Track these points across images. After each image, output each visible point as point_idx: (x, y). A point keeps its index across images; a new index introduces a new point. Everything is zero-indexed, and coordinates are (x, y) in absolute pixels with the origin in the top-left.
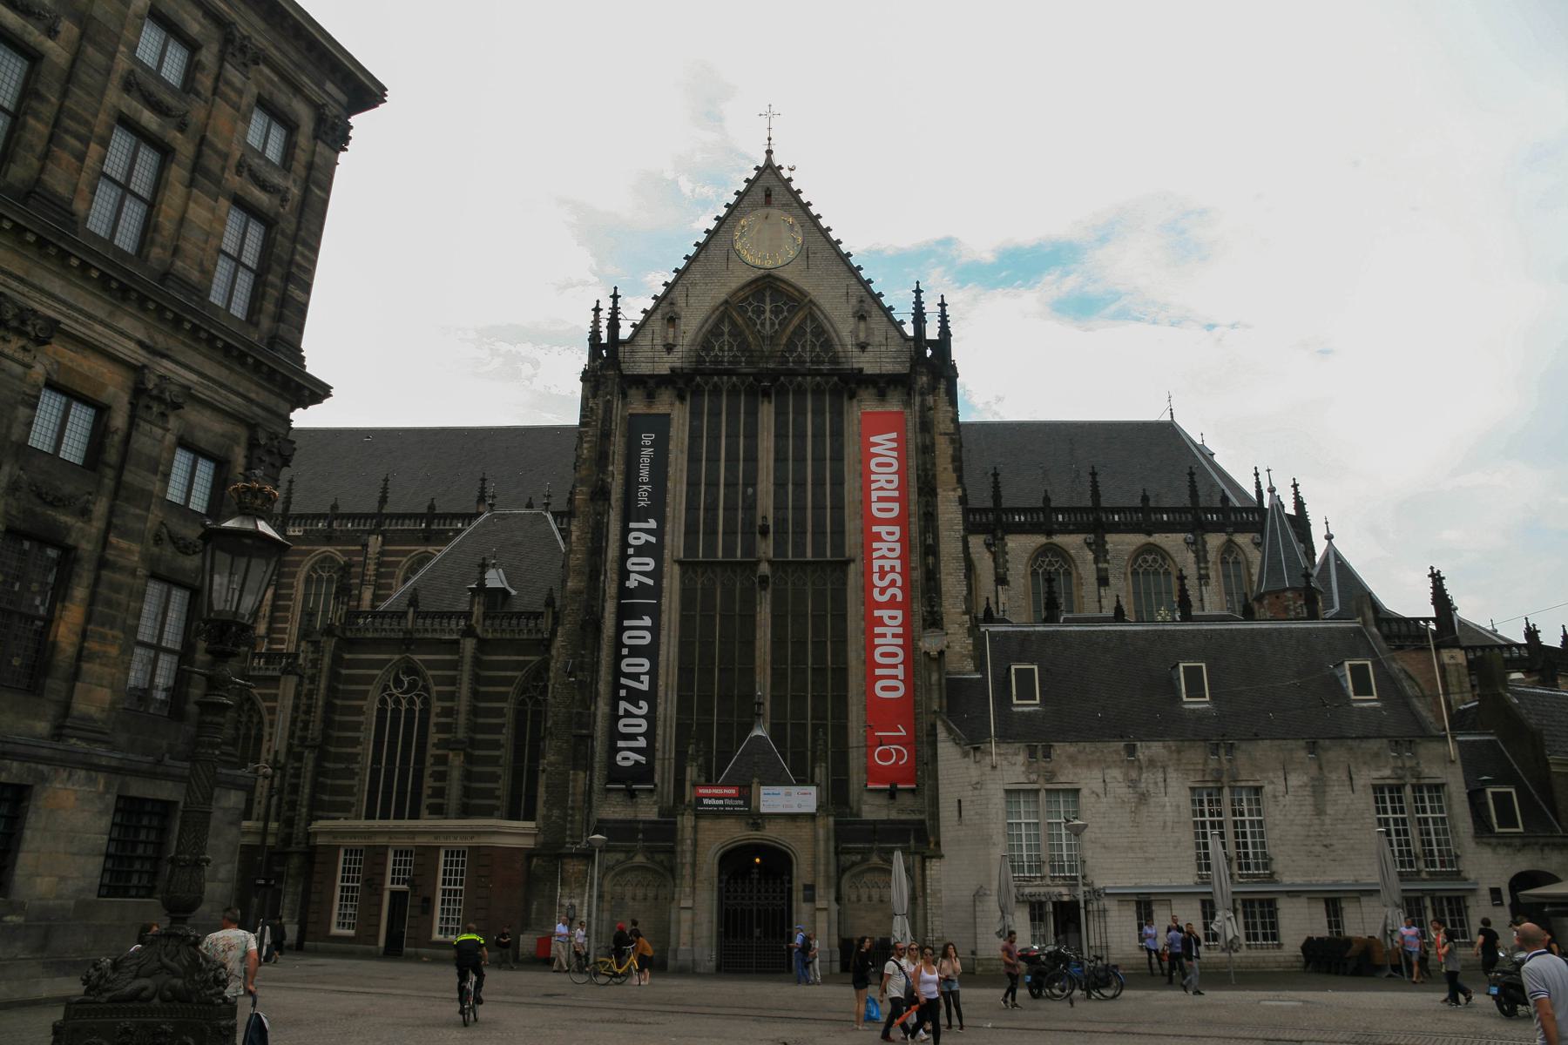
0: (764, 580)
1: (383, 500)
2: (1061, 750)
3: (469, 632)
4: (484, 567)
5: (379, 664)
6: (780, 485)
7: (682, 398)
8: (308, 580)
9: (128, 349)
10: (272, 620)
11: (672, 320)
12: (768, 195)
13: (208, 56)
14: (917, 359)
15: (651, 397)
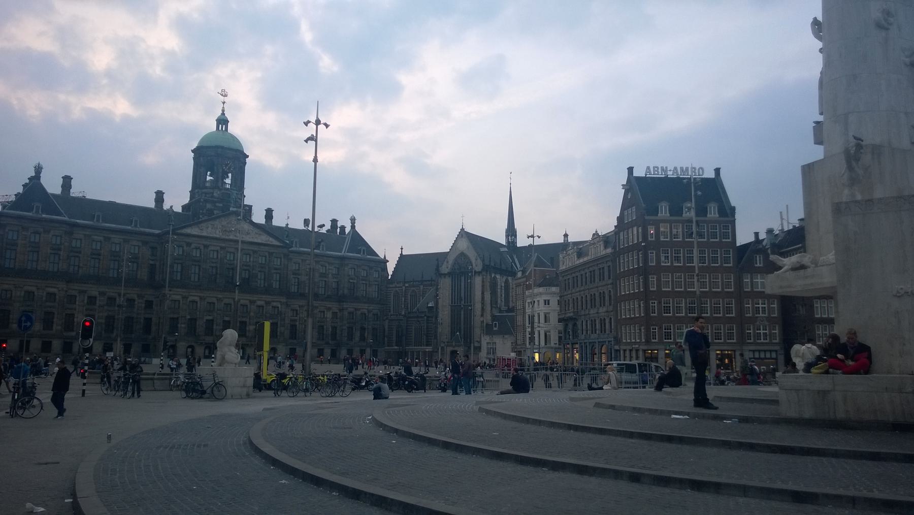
0: (462, 308)
1: (423, 277)
2: (494, 336)
3: (425, 315)
4: (428, 304)
5: (415, 321)
6: (465, 292)
7: (449, 276)
8: (411, 296)
9: (366, 308)
10: (405, 305)
11: (448, 262)
12: (462, 236)
13: (368, 271)
14: (483, 269)
15: (445, 277)
